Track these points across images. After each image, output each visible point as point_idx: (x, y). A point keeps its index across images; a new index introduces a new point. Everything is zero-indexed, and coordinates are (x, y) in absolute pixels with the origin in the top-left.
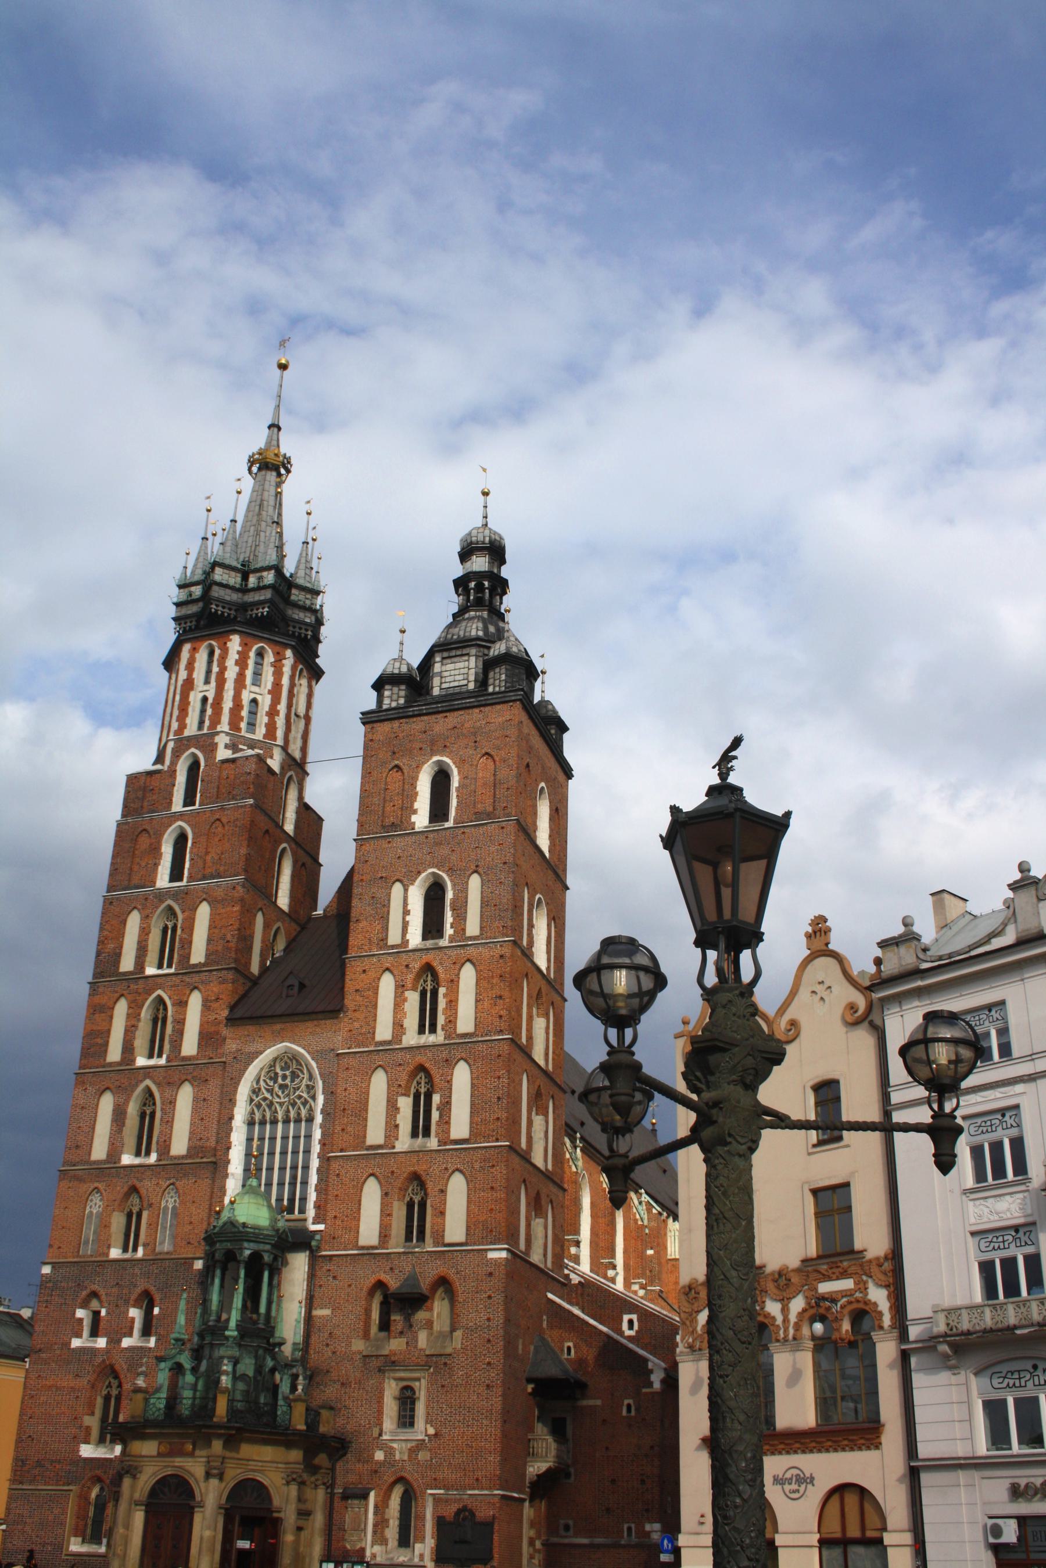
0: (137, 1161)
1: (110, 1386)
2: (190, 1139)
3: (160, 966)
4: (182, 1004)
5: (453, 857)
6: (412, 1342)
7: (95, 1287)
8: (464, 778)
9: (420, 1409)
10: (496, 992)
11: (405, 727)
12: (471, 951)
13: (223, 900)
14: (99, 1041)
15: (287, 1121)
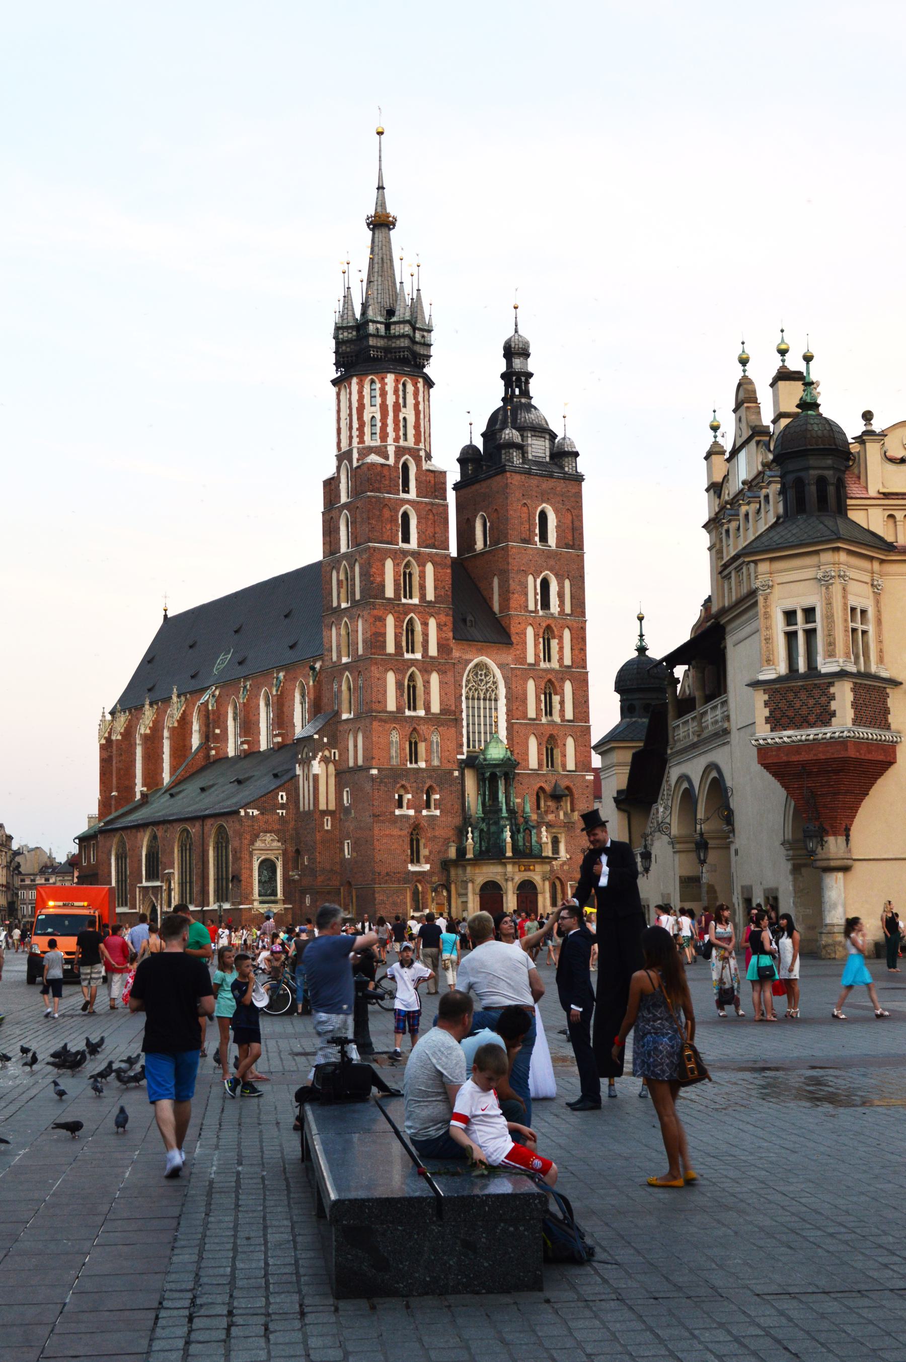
0: (412, 713)
1: (412, 834)
2: (441, 704)
3: (405, 597)
4: (425, 624)
5: (557, 567)
6: (557, 816)
7: (404, 782)
8: (559, 521)
9: (562, 847)
10: (580, 646)
11: (527, 480)
12: (569, 623)
13: (440, 564)
14: (381, 639)
15: (485, 699)
